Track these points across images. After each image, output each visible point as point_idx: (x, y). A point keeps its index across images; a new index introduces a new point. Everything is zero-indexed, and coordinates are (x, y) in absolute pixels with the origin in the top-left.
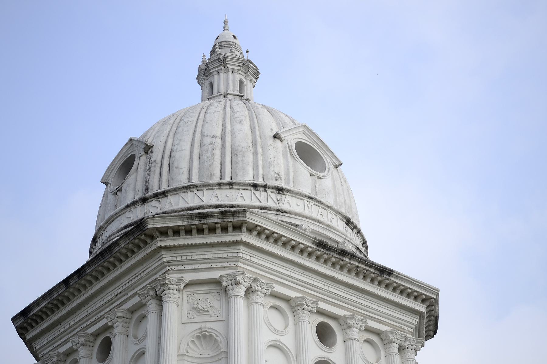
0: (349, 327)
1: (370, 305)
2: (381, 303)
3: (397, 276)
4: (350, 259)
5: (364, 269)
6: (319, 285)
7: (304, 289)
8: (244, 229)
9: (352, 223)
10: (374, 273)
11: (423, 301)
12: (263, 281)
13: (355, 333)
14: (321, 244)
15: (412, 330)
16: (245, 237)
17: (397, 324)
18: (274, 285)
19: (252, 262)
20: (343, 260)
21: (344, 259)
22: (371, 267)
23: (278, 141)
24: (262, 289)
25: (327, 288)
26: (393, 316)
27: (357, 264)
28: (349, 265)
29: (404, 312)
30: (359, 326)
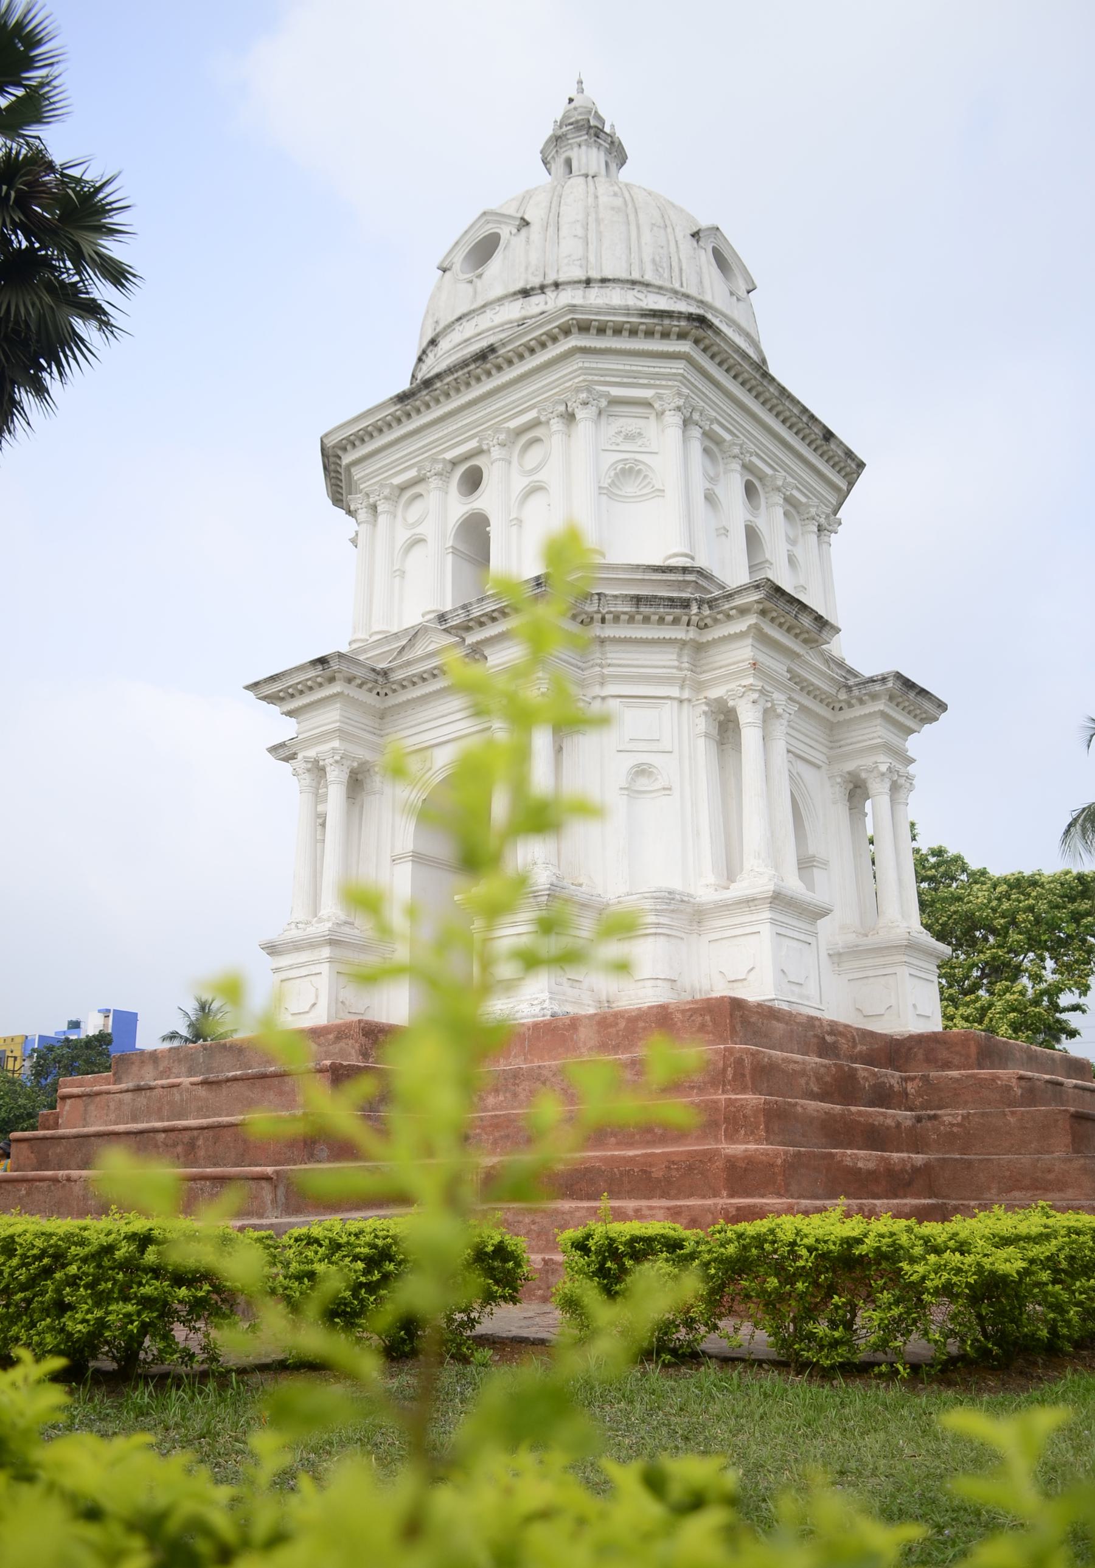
1: (509, 400)
2: (520, 385)
6: (441, 434)
8: (340, 453)
9: (533, 289)
11: (566, 332)
13: (496, 452)
14: (402, 398)
15: (581, 378)
19: (368, 475)
22: (467, 365)
23: (448, 274)
25: (450, 429)
26: (544, 386)
29: (555, 367)
30: (495, 441)
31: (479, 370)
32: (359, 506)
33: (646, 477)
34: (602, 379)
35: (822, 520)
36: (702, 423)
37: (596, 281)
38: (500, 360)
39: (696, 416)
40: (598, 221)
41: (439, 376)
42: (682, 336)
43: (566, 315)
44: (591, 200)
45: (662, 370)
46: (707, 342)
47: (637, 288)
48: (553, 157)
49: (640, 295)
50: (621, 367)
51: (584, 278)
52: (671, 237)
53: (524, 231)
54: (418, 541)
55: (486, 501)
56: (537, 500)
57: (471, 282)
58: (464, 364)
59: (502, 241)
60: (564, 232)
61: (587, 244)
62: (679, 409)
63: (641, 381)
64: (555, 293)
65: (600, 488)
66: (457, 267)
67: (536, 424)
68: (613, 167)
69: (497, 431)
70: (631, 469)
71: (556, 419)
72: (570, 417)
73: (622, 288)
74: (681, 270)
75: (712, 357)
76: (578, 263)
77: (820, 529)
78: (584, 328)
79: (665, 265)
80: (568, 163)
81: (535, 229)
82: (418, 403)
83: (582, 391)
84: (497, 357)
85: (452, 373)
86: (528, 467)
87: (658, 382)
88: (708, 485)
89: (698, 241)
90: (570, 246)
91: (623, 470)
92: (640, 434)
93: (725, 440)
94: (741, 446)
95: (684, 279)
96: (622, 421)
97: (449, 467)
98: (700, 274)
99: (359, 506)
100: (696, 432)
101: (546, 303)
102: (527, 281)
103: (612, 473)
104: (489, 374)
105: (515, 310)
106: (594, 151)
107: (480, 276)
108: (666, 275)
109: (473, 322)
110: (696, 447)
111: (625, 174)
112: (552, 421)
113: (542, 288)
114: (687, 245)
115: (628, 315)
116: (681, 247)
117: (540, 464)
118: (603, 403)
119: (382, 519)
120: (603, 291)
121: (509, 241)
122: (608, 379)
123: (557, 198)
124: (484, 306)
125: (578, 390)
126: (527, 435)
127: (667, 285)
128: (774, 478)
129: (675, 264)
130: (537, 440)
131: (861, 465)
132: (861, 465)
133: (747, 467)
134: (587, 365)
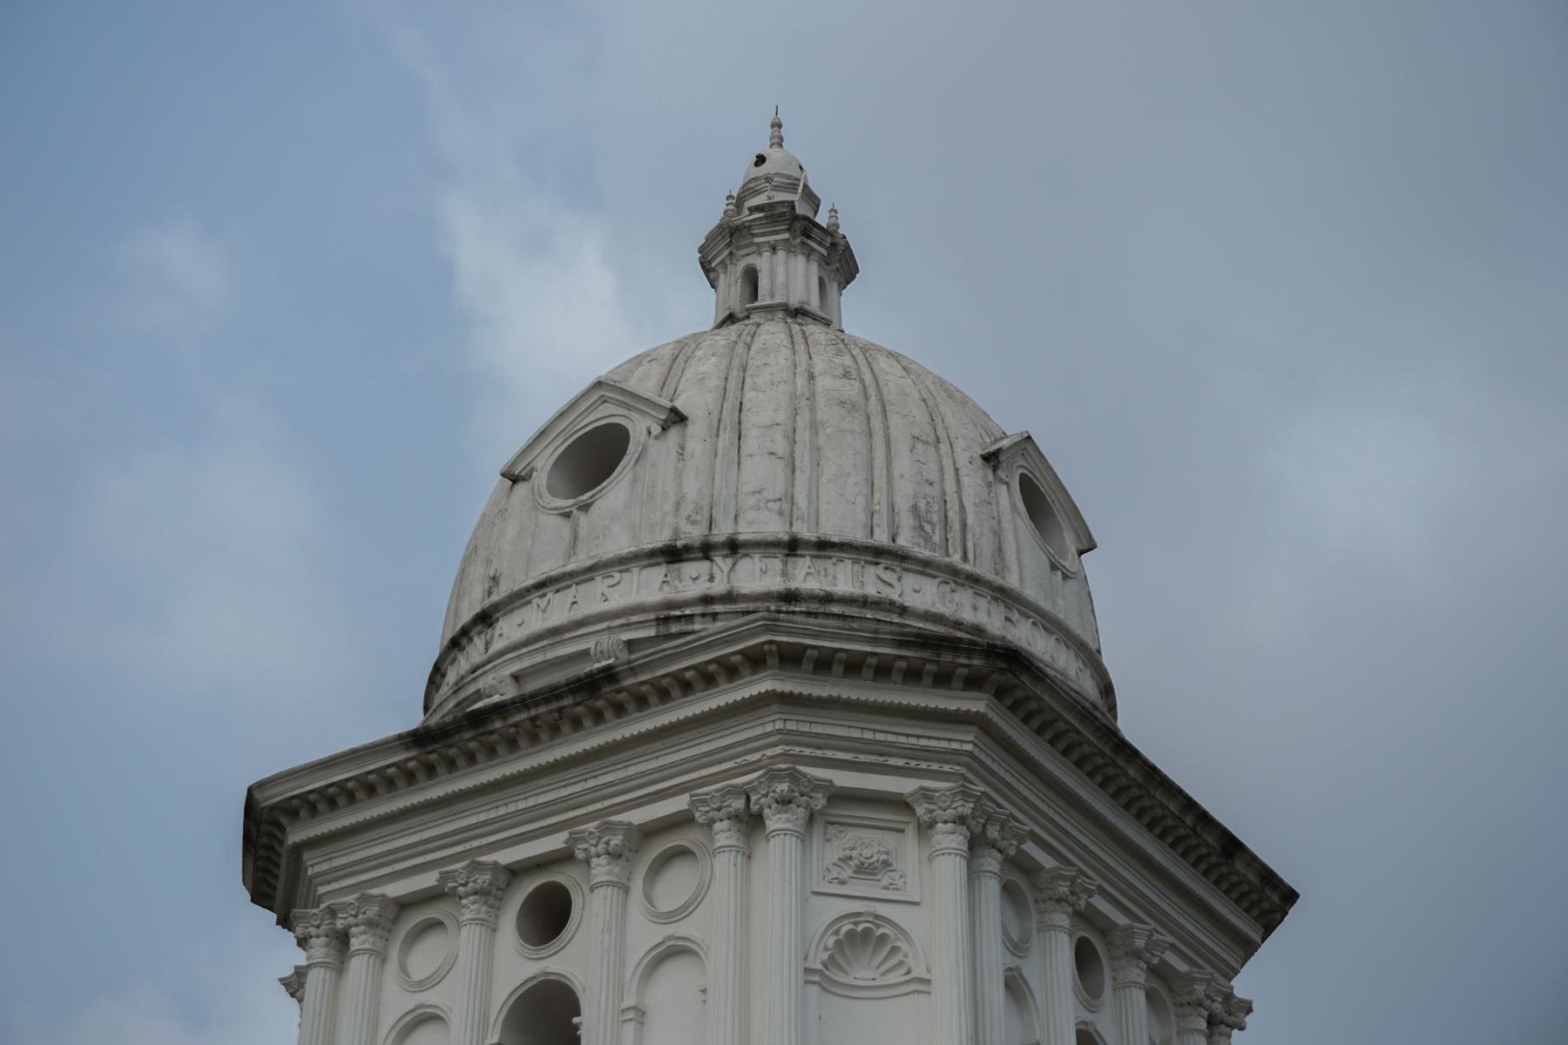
0: (587, 862)
1: (632, 771)
2: (658, 745)
3: (632, 669)
4: (504, 718)
5: (550, 712)
6: (492, 814)
7: (467, 846)
8: (284, 820)
9: (687, 548)
10: (578, 704)
11: (756, 661)
12: (350, 898)
13: (602, 869)
15: (778, 750)
16: (296, 835)
17: (730, 764)
18: (374, 891)
20: (491, 732)
21: (490, 728)
22: (559, 697)
23: (522, 488)
24: (356, 916)
25: (512, 808)
27: (523, 716)
28: (512, 730)
30: (601, 847)
31: (580, 709)
32: (313, 931)
33: (895, 950)
34: (819, 753)
35: (1217, 1007)
36: (1003, 844)
37: (808, 544)
38: (622, 696)
39: (993, 832)
40: (815, 427)
41: (500, 709)
42: (973, 682)
43: (757, 634)
44: (801, 382)
45: (933, 743)
46: (1019, 694)
47: (884, 562)
48: (722, 262)
49: (888, 576)
50: (856, 734)
51: (786, 538)
52: (947, 463)
53: (674, 433)
54: (425, 1018)
55: (575, 958)
56: (675, 975)
57: (567, 515)
58: (553, 693)
59: (631, 447)
60: (751, 442)
61: (790, 472)
62: (961, 820)
63: (892, 761)
64: (729, 561)
65: (807, 970)
66: (541, 478)
67: (682, 821)
68: (832, 287)
69: (608, 828)
70: (867, 933)
71: (725, 824)
72: (751, 823)
73: (856, 562)
74: (964, 526)
75: (1026, 720)
76: (776, 506)
77: (1212, 1022)
78: (790, 658)
79: (935, 518)
80: (751, 277)
81: (697, 429)
82: (453, 752)
83: (781, 779)
84: (619, 691)
85: (527, 707)
86: (665, 905)
87: (924, 765)
88: (1011, 961)
89: (995, 469)
90: (761, 473)
91: (851, 934)
92: (886, 864)
93: (1041, 868)
94: (1073, 880)
95: (970, 545)
96: (852, 835)
97: (503, 878)
98: (998, 534)
99: (313, 931)
100: (992, 862)
101: (711, 579)
102: (676, 531)
103: (831, 941)
104: (598, 717)
105: (648, 587)
106: (799, 263)
107: (585, 507)
108: (937, 538)
109: (568, 596)
110: (991, 889)
111: (858, 311)
112: (717, 826)
113: (706, 550)
114: (974, 478)
115: (875, 641)
116: (966, 481)
117: (686, 905)
118: (820, 801)
119: (358, 966)
120: (821, 564)
121: (645, 448)
122: (829, 754)
123: (737, 378)
124: (592, 569)
125: (773, 776)
126: (661, 844)
127: (937, 556)
128: (1129, 932)
129: (953, 516)
130: (682, 853)
131: (1290, 896)
132: (1290, 896)
133: (1086, 917)
134: (791, 726)
